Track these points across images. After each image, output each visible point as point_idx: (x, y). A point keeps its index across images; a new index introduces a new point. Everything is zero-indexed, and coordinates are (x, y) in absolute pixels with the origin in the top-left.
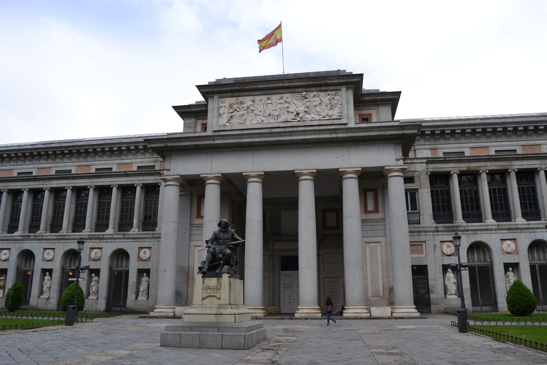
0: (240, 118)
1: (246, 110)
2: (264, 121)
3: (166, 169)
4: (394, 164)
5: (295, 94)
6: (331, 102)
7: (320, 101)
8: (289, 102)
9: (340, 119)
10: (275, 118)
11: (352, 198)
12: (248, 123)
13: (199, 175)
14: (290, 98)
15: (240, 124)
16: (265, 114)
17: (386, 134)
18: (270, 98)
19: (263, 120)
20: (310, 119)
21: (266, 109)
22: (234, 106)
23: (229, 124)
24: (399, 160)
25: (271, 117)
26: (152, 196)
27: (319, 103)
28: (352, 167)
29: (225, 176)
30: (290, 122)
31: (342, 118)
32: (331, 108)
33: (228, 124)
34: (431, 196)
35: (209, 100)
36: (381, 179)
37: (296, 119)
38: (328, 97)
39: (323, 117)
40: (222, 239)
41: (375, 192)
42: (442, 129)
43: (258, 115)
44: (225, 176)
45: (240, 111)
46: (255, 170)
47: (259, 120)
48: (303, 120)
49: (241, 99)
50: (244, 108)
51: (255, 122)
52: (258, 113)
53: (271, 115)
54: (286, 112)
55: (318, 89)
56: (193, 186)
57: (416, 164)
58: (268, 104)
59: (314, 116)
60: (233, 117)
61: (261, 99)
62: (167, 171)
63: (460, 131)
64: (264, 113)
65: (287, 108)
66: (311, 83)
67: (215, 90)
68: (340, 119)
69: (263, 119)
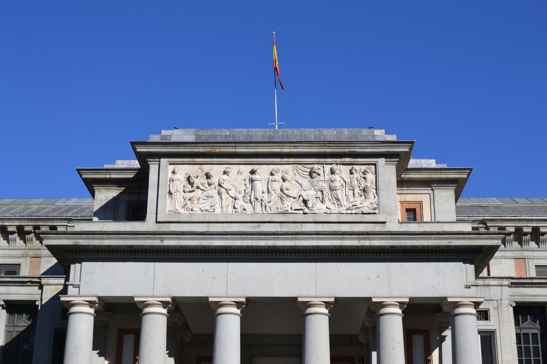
0: (204, 201)
3: (73, 285)
4: (461, 294)
5: (300, 166)
6: (360, 185)
7: (342, 181)
8: (289, 179)
9: (375, 213)
10: (265, 206)
11: (393, 349)
12: (218, 210)
13: (132, 298)
14: (291, 173)
15: (205, 212)
18: (258, 171)
19: (246, 208)
20: (326, 211)
23: (186, 212)
24: (470, 288)
26: (19, 324)
27: (340, 185)
28: (393, 296)
30: (291, 215)
31: (377, 211)
32: (360, 194)
33: (182, 211)
34: (517, 344)
35: (151, 166)
36: (436, 314)
37: (302, 210)
38: (356, 175)
39: (347, 209)
41: (426, 334)
42: (535, 225)
44: (174, 300)
46: (229, 294)
48: (313, 212)
49: (207, 168)
54: (284, 196)
55: (339, 160)
56: (111, 313)
57: (491, 288)
59: (332, 206)
60: (193, 199)
61: (241, 171)
62: (73, 287)
64: (247, 196)
65: (286, 190)
66: (328, 150)
68: (375, 213)
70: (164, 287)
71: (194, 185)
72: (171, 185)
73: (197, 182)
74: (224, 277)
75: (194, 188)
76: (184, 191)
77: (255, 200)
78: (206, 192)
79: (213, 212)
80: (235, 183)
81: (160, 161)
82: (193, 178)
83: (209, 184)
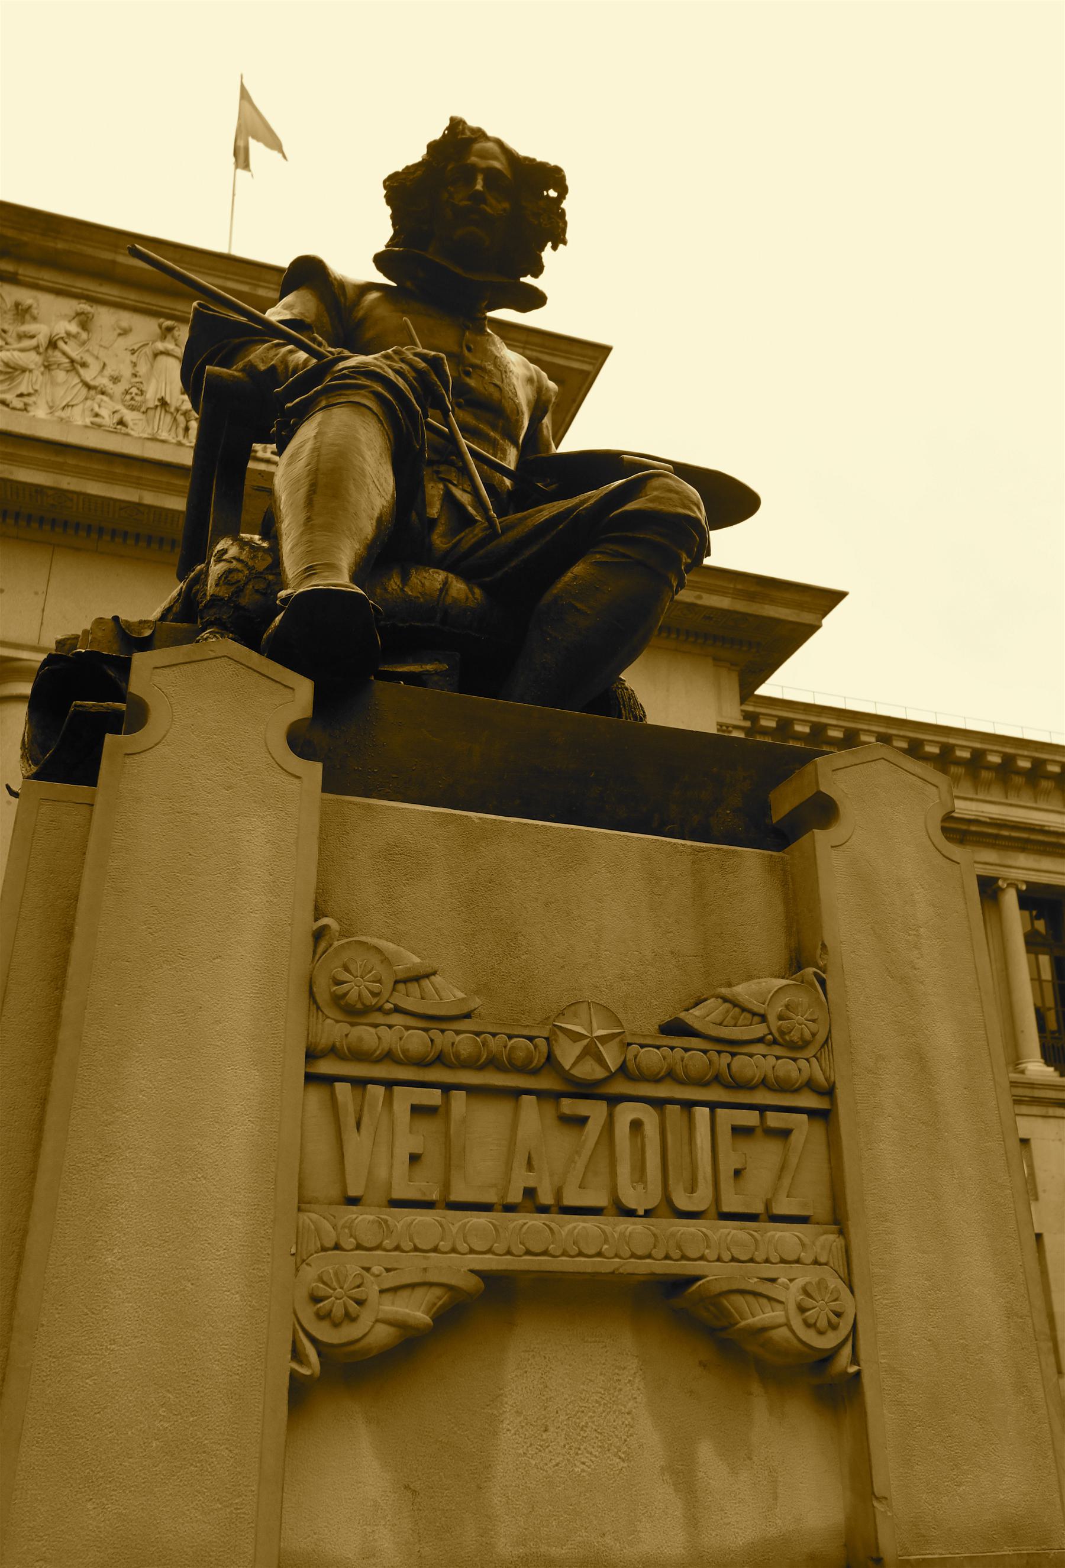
1: (41, 350)
2: (130, 424)
12: (40, 412)
16: (138, 398)
17: (699, 602)
21: (149, 380)
25: (168, 419)
43: (103, 393)
47: (104, 412)
50: (33, 342)
51: (79, 417)
52: (103, 381)
53: (172, 410)
58: (162, 359)
61: (124, 324)
63: (807, 730)
69: (129, 416)
74: (36, 593)
77: (158, 404)
79: (20, 410)
80: (102, 353)
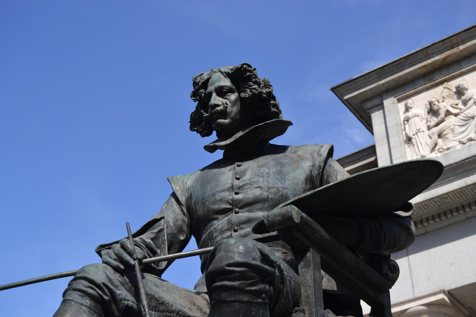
0: (463, 129)
15: (468, 144)
22: (442, 105)
29: (457, 300)
40: (224, 212)
44: (457, 300)
45: (462, 111)
60: (445, 133)
67: (383, 82)
70: (429, 279)
71: (440, 111)
72: (407, 126)
73: (444, 106)
75: (442, 115)
76: (429, 128)
78: (463, 114)
81: (382, 104)
82: (436, 103)
83: (465, 103)
